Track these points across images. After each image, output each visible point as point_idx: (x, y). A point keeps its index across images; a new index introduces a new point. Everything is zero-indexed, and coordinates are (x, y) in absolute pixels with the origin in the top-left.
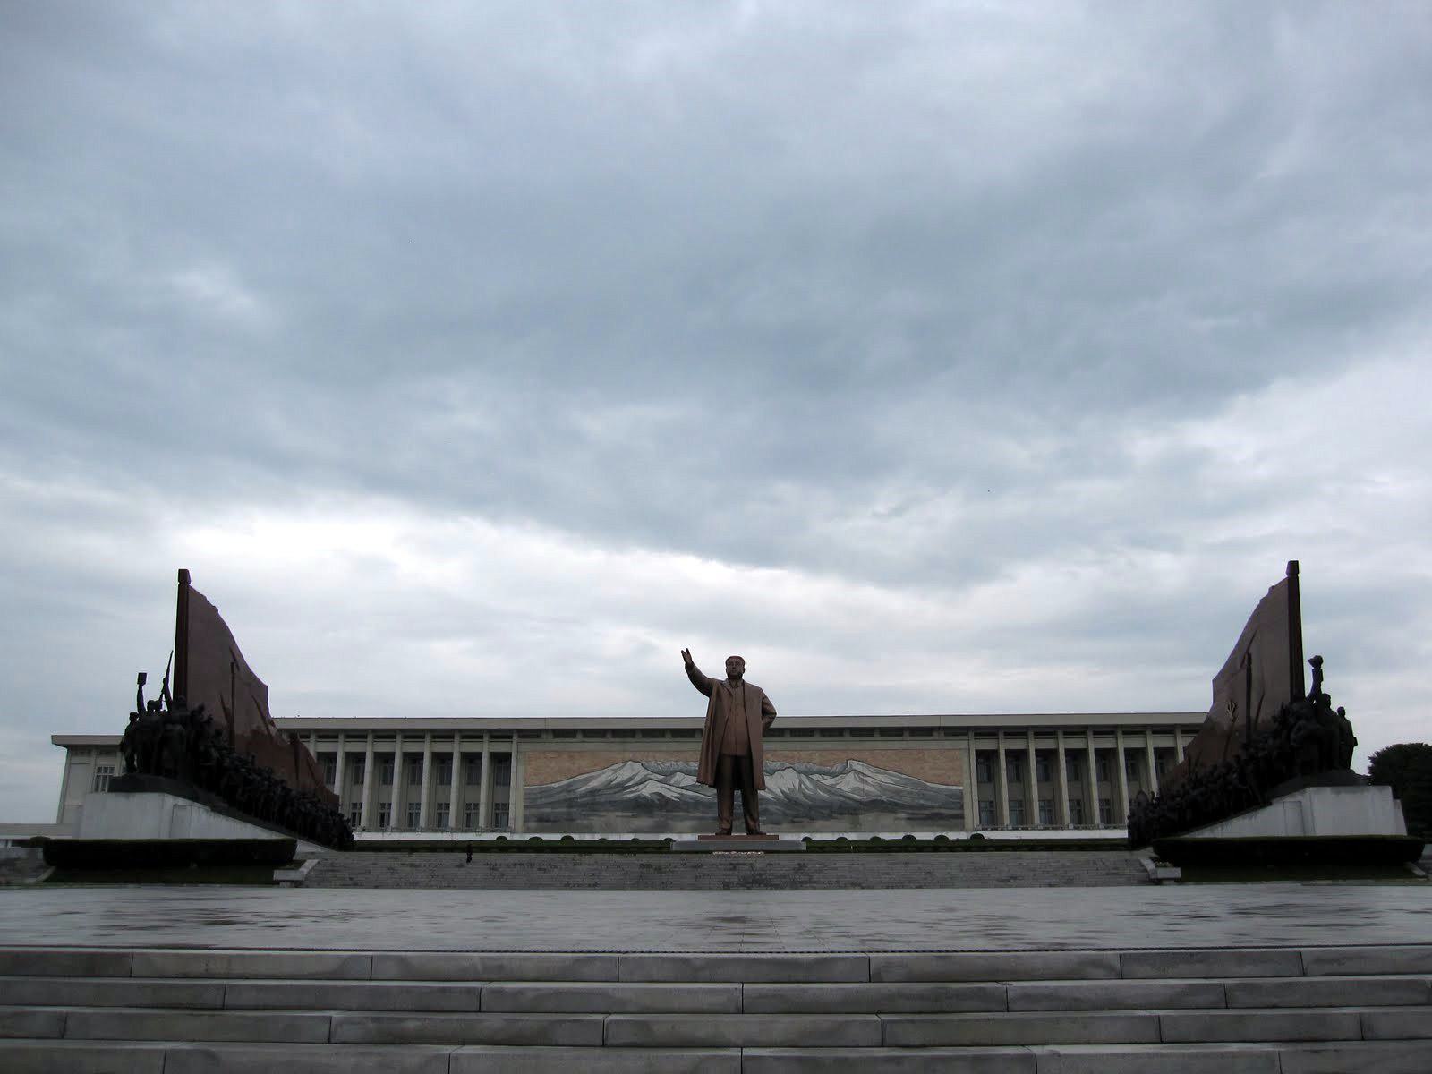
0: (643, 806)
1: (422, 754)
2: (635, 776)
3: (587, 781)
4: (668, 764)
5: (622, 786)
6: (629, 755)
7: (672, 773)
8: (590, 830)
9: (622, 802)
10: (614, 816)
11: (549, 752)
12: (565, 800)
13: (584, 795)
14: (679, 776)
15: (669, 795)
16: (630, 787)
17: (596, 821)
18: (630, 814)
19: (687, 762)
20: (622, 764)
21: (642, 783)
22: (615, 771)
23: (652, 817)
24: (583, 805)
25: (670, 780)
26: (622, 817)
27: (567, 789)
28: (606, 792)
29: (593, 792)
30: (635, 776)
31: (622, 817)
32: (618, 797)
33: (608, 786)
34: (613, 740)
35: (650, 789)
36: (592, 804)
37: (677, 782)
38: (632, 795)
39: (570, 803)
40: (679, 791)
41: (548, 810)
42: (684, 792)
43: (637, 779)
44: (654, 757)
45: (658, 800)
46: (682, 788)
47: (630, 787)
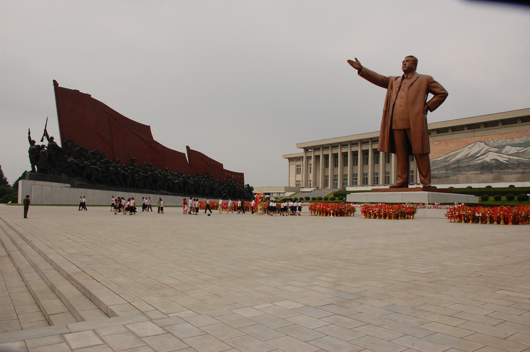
0: (485, 167)
1: (368, 150)
2: (481, 150)
3: (455, 155)
4: (501, 141)
5: (474, 157)
6: (478, 139)
7: (504, 147)
8: (457, 182)
9: (474, 166)
10: (471, 174)
11: (436, 141)
12: (444, 166)
13: (454, 163)
14: (507, 148)
15: (501, 160)
16: (478, 157)
17: (461, 177)
18: (479, 172)
19: (512, 139)
20: (473, 144)
21: (485, 154)
22: (470, 148)
23: (492, 173)
24: (453, 169)
25: (502, 151)
26: (475, 174)
27: (445, 160)
28: (465, 160)
29: (458, 161)
30: (481, 150)
31: (475, 174)
32: (471, 163)
33: (466, 157)
34: (468, 131)
35: (489, 158)
36: (459, 167)
37: (506, 152)
38: (479, 161)
39: (446, 168)
40: (508, 157)
41: (436, 172)
42: (511, 157)
43: (482, 152)
44: (492, 138)
45: (495, 163)
46: (509, 155)
47: (478, 157)
